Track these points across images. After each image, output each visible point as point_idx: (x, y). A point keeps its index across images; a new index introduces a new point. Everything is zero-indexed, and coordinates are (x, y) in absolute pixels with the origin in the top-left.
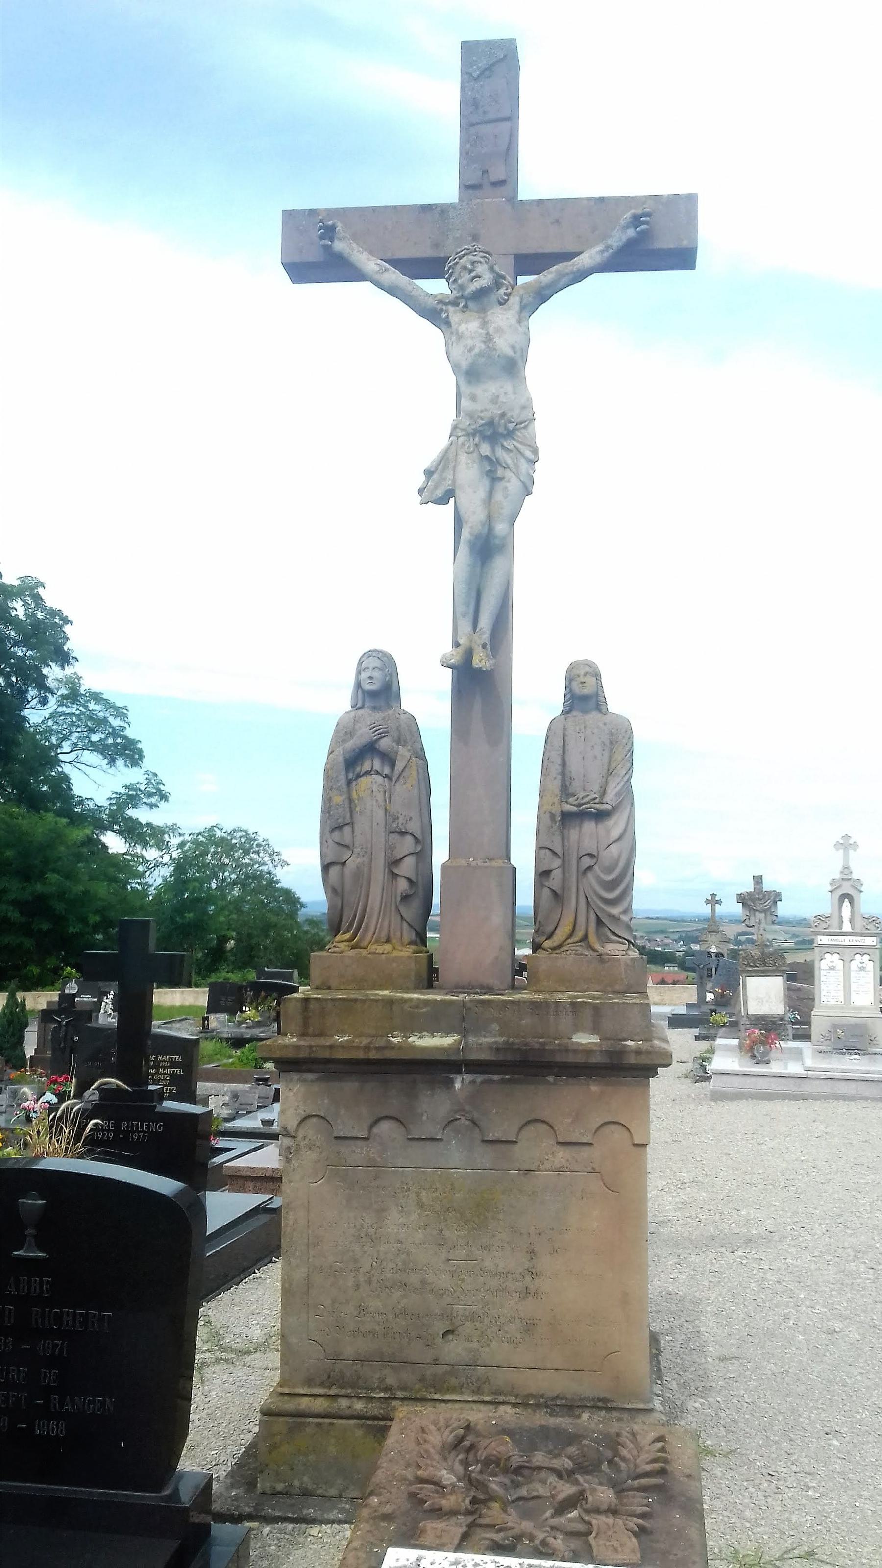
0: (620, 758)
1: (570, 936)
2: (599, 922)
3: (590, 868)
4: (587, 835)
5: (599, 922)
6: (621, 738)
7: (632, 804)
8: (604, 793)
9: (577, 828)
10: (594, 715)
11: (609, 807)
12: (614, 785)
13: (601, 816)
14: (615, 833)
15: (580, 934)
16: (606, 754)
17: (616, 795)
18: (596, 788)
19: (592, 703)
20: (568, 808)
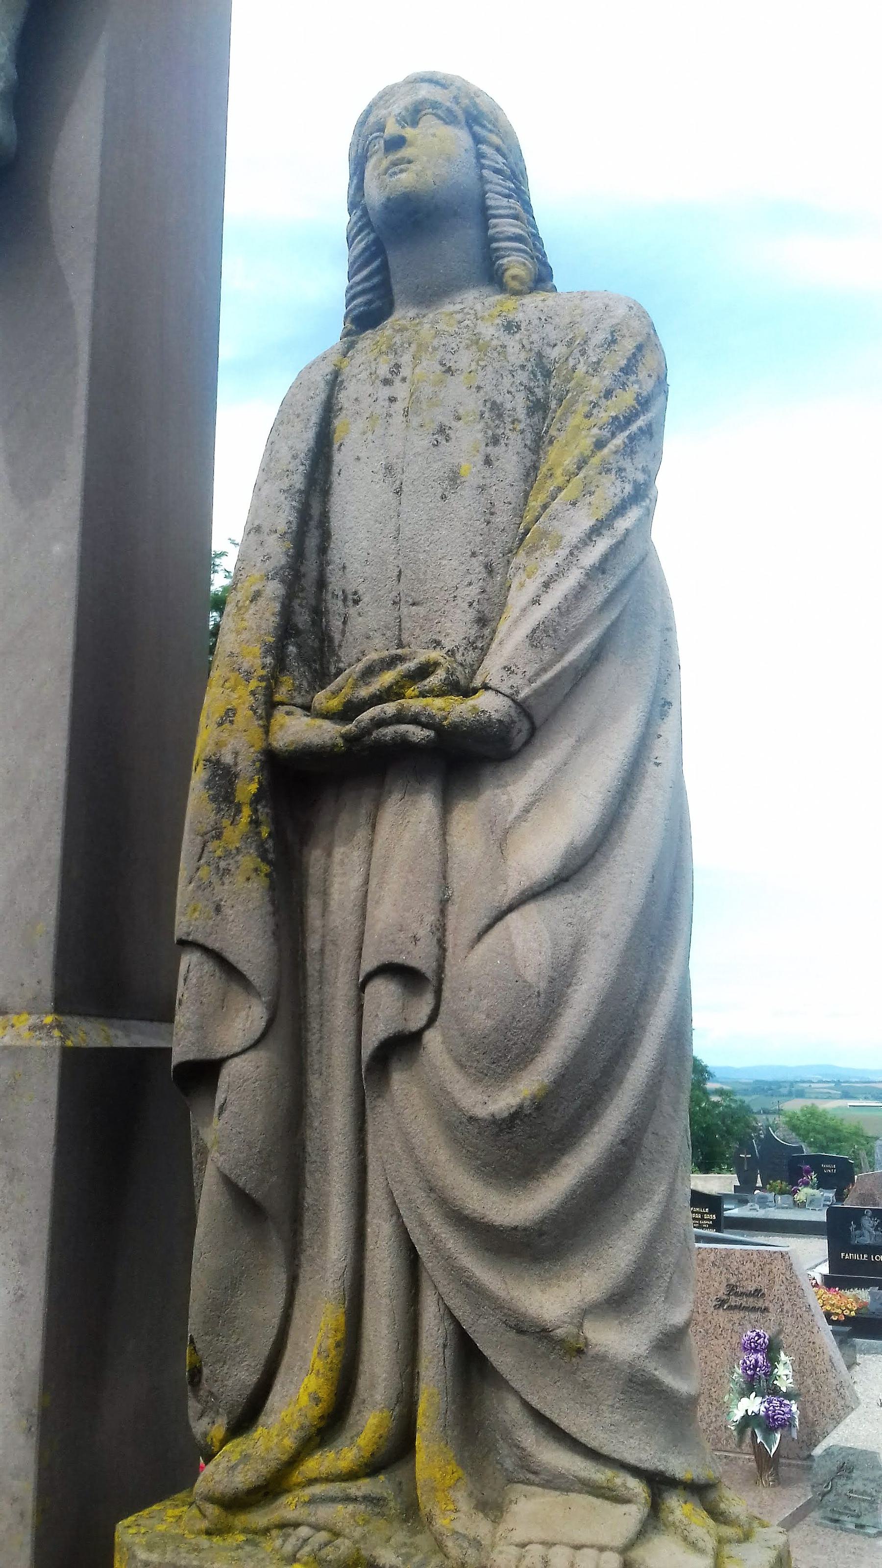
0: (569, 461)
1: (331, 1424)
2: (470, 1364)
3: (402, 1046)
4: (386, 867)
5: (470, 1364)
6: (582, 368)
7: (661, 705)
8: (480, 645)
9: (362, 835)
10: (476, 306)
11: (490, 705)
12: (532, 586)
13: (464, 759)
14: (539, 851)
15: (370, 1423)
16: (510, 460)
17: (534, 639)
18: (457, 628)
19: (456, 247)
20: (296, 729)
